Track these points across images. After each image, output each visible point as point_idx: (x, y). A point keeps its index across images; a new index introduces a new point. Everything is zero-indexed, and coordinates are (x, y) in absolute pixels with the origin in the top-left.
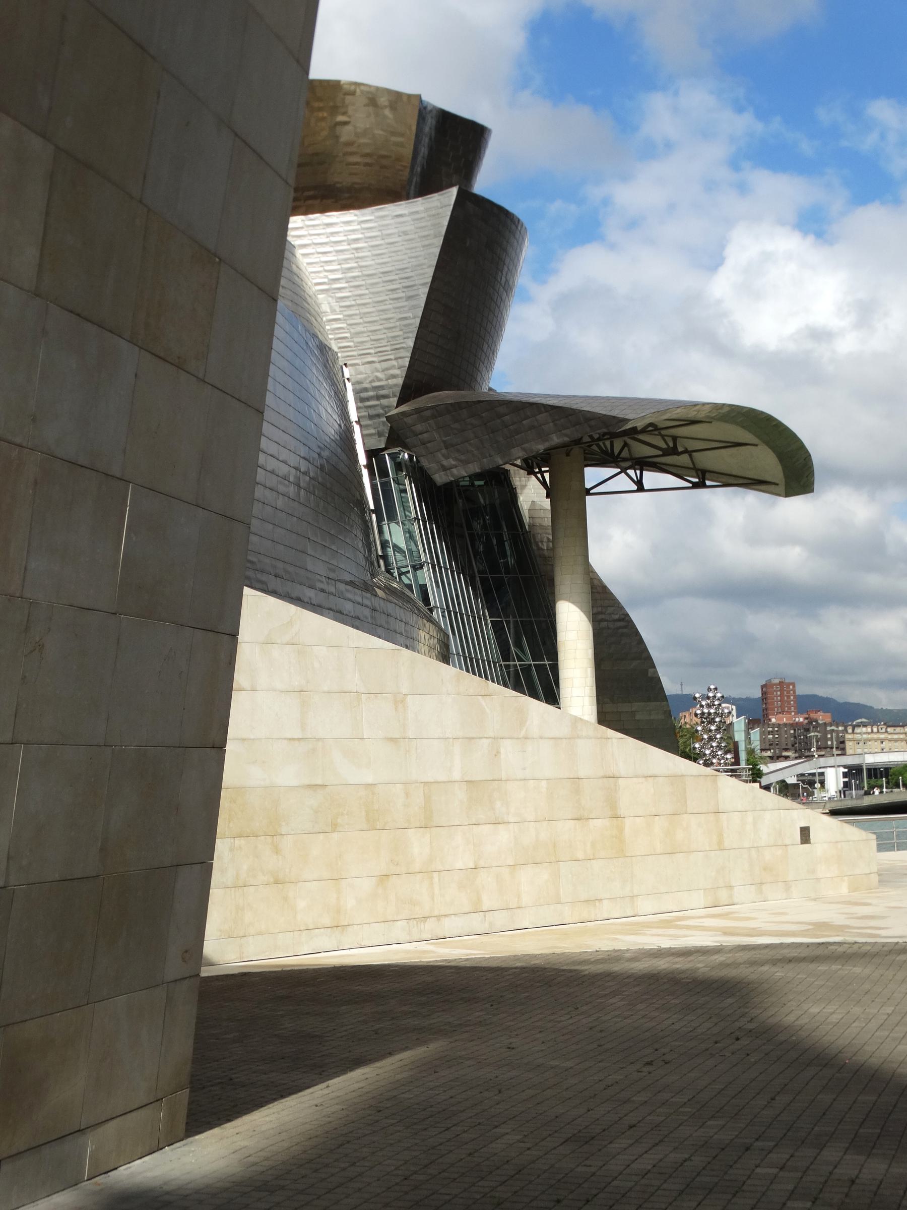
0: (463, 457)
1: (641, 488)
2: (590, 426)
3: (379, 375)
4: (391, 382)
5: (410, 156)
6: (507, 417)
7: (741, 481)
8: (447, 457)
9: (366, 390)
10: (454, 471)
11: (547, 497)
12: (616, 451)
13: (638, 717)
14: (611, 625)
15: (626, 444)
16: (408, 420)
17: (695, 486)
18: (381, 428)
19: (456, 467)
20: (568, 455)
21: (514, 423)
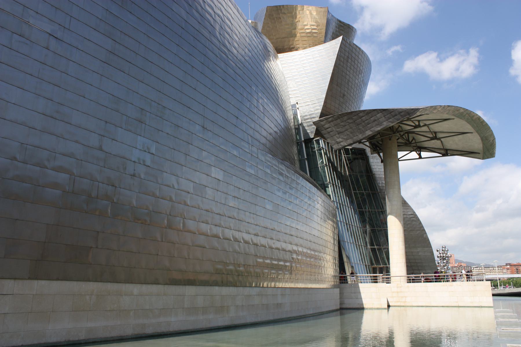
0: (345, 137)
1: (420, 157)
2: (401, 116)
3: (312, 110)
4: (316, 112)
5: (324, 32)
6: (364, 118)
7: (463, 153)
8: (338, 138)
9: (306, 116)
10: (342, 143)
11: (382, 162)
12: (410, 140)
13: (420, 254)
14: (408, 216)
15: (414, 139)
16: (322, 123)
17: (444, 155)
18: (312, 130)
19: (342, 142)
20: (390, 140)
21: (367, 120)
